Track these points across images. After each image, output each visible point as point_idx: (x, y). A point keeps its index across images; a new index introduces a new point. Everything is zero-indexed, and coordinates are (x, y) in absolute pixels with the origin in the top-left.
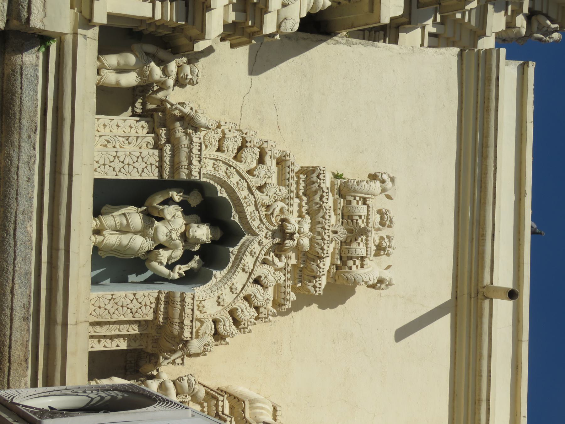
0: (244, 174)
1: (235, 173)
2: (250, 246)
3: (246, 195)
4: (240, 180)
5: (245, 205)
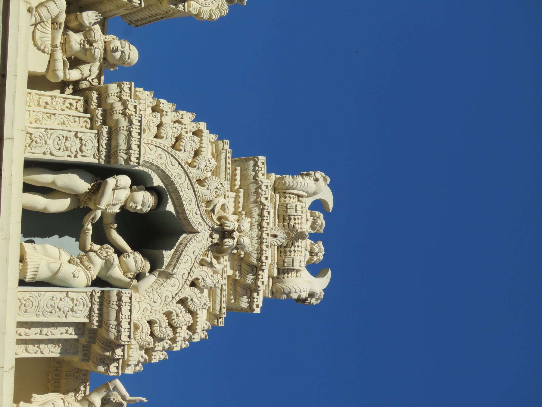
2: (188, 245)
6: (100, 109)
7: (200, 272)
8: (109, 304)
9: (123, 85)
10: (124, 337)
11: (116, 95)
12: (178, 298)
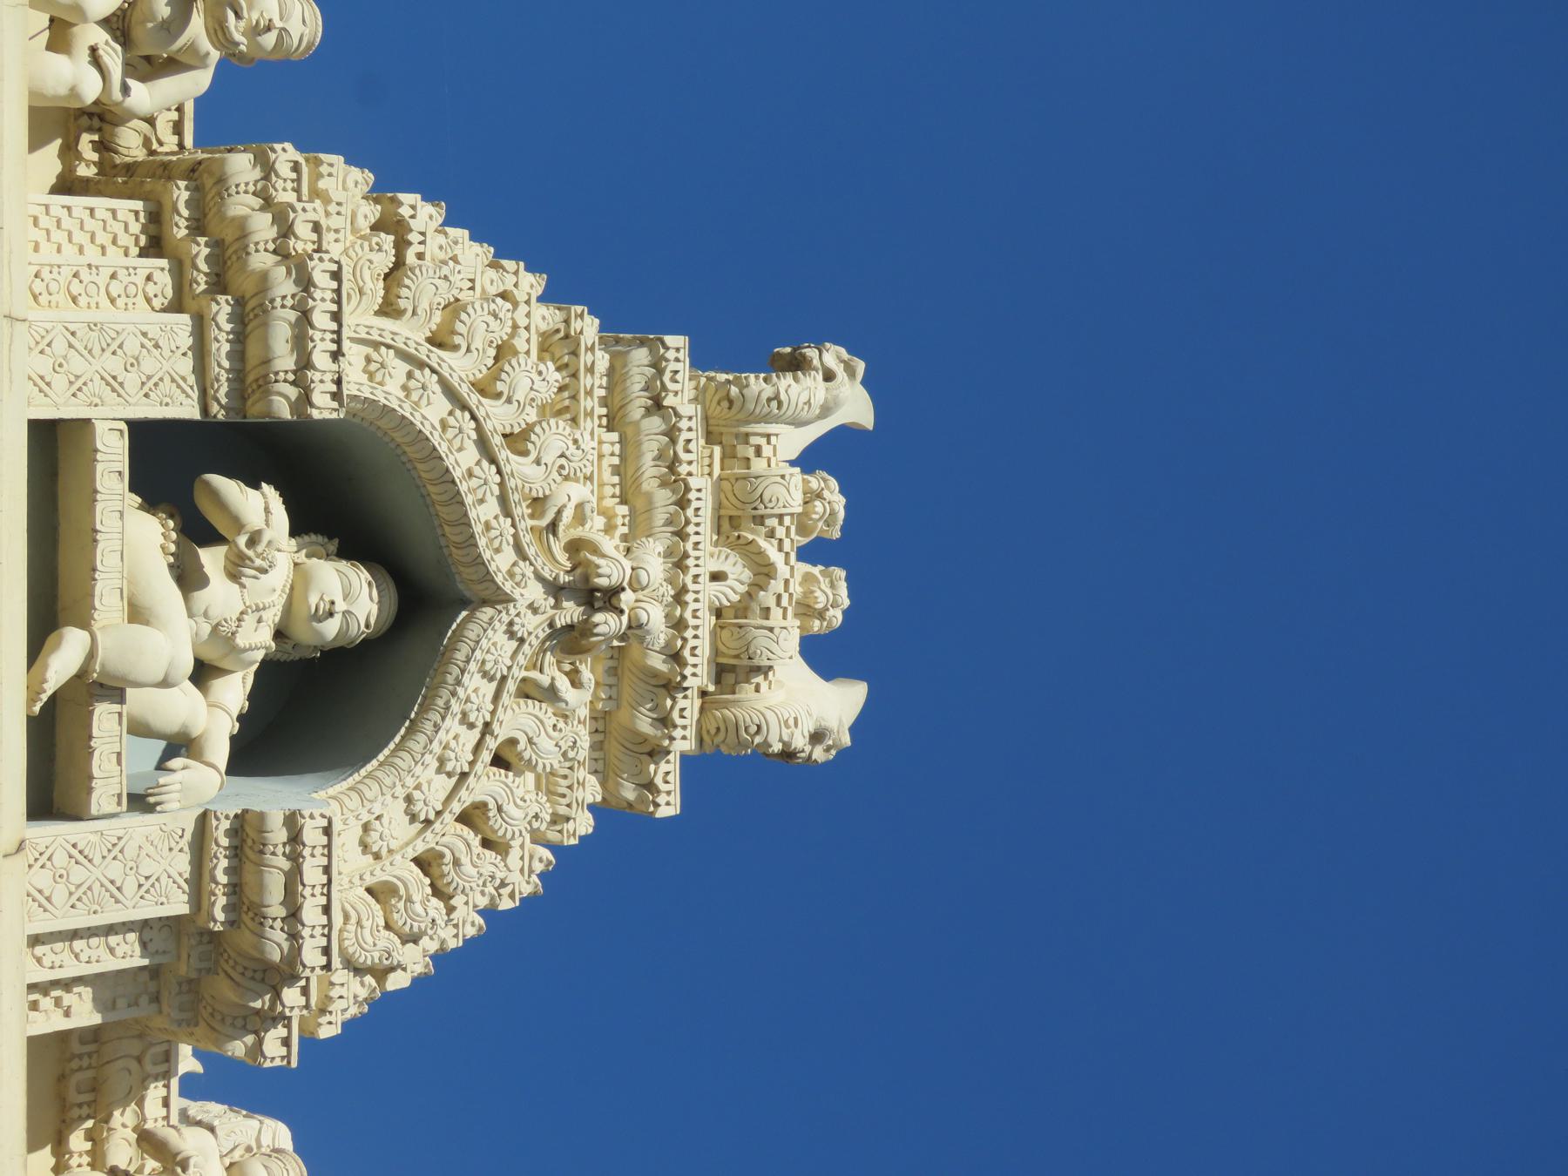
0: (464, 390)
1: (437, 388)
2: (484, 642)
3: (472, 464)
4: (451, 413)
6: (202, 240)
7: (517, 720)
8: (262, 852)
9: (273, 156)
10: (311, 955)
11: (251, 188)
12: (457, 808)
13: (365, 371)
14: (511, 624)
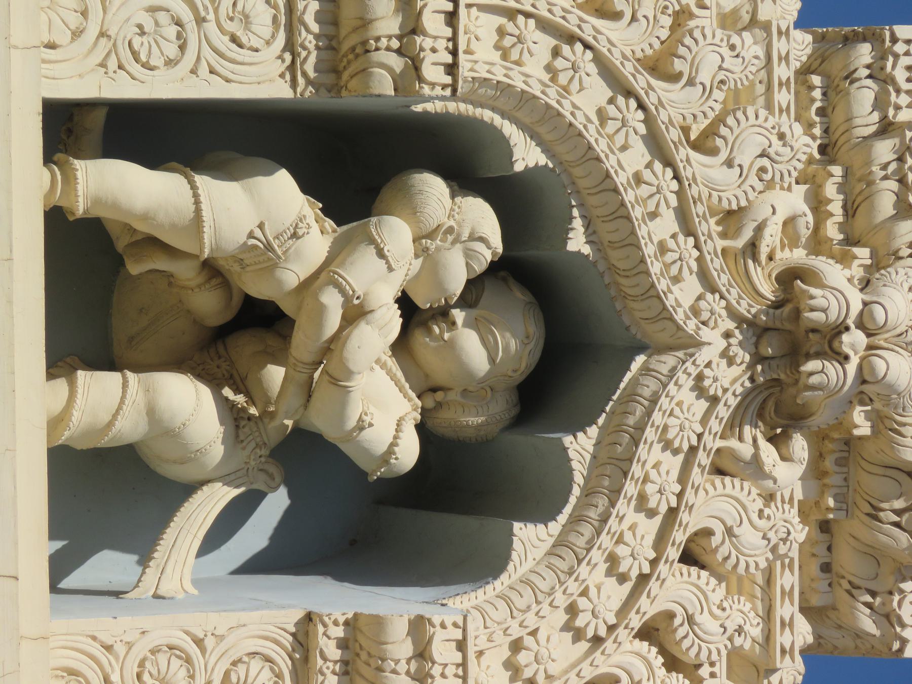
0: (628, 70)
1: (592, 68)
2: (664, 401)
4: (611, 101)
5: (637, 213)
7: (714, 505)
12: (636, 622)
13: (497, 47)
14: (700, 378)
